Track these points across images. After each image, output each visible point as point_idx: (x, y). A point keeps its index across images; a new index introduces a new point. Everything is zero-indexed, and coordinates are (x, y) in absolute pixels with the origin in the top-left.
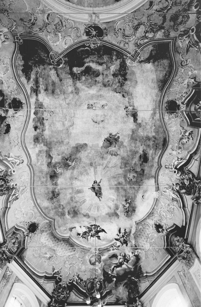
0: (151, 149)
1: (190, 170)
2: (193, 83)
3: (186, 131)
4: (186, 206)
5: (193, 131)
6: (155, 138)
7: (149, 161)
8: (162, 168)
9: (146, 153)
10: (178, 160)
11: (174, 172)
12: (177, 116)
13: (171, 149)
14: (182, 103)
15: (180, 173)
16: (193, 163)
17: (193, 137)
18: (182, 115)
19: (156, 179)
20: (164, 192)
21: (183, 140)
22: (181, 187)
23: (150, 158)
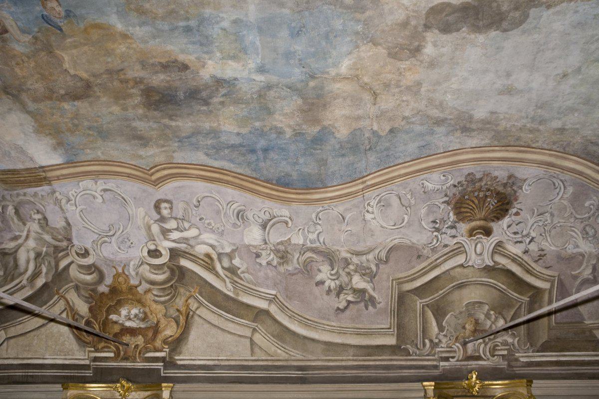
0: (243, 121)
1: (196, 318)
2: (575, 277)
3: (371, 276)
4: (12, 331)
5: (374, 305)
6: (318, 140)
7: (166, 121)
8: (150, 188)
9: (216, 100)
10: (220, 255)
11: (153, 247)
12: (437, 230)
13: (267, 217)
14: (499, 244)
15: (161, 278)
16: (230, 327)
17: (348, 312)
18: (447, 250)
19: (65, 172)
20: (17, 212)
21: (325, 268)
22: (94, 290)
23: (185, 125)
